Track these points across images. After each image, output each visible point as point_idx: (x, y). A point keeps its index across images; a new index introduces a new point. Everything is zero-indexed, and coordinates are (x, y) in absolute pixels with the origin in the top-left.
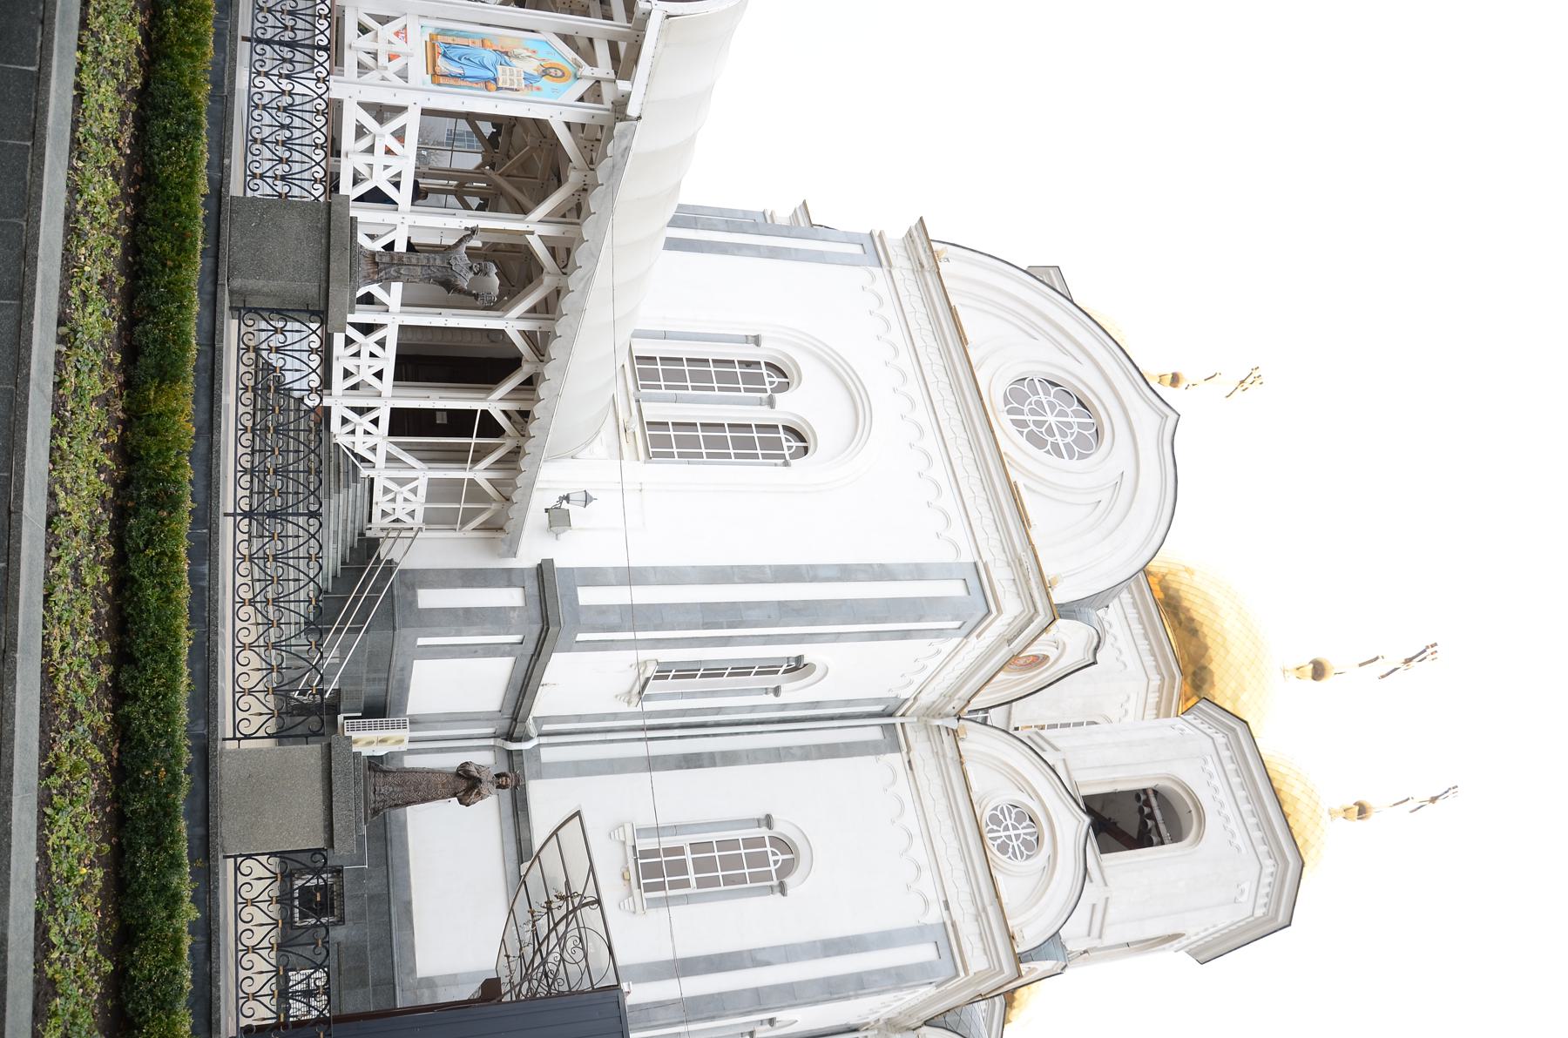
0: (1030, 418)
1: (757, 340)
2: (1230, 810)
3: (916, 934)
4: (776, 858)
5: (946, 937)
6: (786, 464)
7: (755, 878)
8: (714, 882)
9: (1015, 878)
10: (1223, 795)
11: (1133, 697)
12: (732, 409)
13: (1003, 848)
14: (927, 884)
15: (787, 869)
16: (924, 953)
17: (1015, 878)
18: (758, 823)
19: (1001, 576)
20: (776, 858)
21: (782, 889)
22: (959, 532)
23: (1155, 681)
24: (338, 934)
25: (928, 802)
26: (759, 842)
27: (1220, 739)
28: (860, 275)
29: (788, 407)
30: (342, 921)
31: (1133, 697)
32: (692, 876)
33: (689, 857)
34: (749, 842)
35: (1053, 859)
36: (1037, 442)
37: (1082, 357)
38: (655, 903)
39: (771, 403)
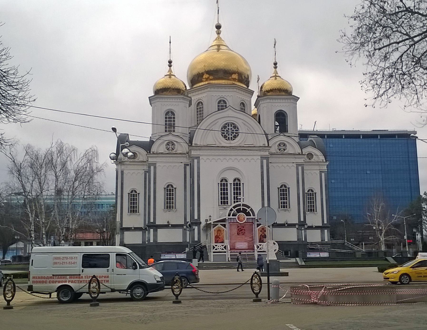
0: (230, 136)
1: (219, 184)
2: (282, 104)
3: (297, 169)
4: (283, 188)
5: (298, 165)
6: (243, 184)
7: (286, 191)
8: (286, 198)
9: (289, 150)
10: (279, 104)
11: (237, 95)
12: (231, 190)
13: (284, 150)
14: (291, 165)
15: (285, 187)
16: (300, 168)
17: (289, 150)
18: (279, 190)
19: (263, 153)
20: (283, 188)
21: (289, 188)
22: (255, 158)
23: (235, 90)
24: (292, 251)
25: (277, 161)
26: (281, 189)
27: (268, 101)
28: (201, 161)
29: (231, 181)
30: (290, 251)
31: (237, 95)
32: (285, 201)
33: (282, 201)
34: (281, 192)
35: (287, 142)
36: (235, 137)
37: (218, 121)
38: (289, 208)
39: (231, 184)
